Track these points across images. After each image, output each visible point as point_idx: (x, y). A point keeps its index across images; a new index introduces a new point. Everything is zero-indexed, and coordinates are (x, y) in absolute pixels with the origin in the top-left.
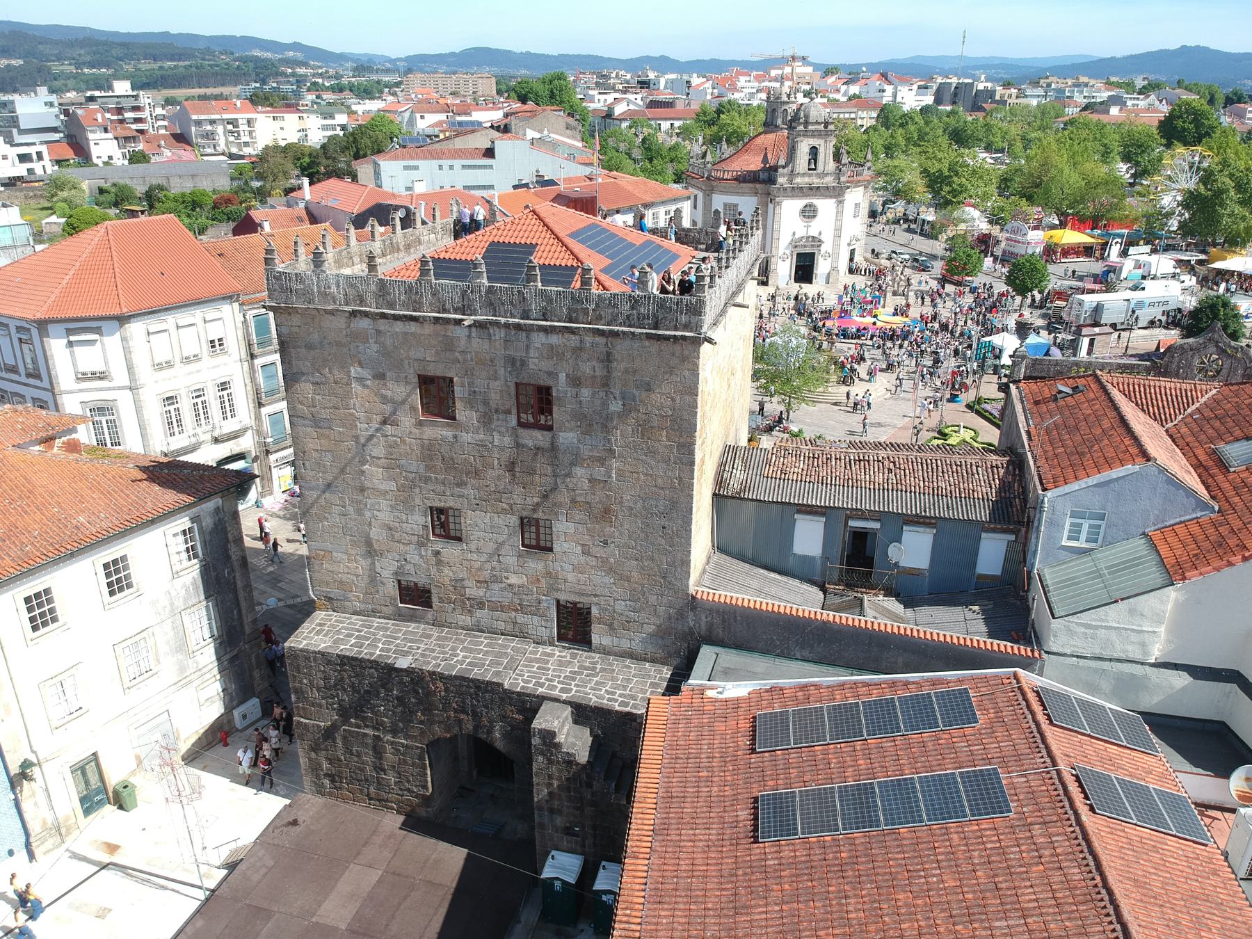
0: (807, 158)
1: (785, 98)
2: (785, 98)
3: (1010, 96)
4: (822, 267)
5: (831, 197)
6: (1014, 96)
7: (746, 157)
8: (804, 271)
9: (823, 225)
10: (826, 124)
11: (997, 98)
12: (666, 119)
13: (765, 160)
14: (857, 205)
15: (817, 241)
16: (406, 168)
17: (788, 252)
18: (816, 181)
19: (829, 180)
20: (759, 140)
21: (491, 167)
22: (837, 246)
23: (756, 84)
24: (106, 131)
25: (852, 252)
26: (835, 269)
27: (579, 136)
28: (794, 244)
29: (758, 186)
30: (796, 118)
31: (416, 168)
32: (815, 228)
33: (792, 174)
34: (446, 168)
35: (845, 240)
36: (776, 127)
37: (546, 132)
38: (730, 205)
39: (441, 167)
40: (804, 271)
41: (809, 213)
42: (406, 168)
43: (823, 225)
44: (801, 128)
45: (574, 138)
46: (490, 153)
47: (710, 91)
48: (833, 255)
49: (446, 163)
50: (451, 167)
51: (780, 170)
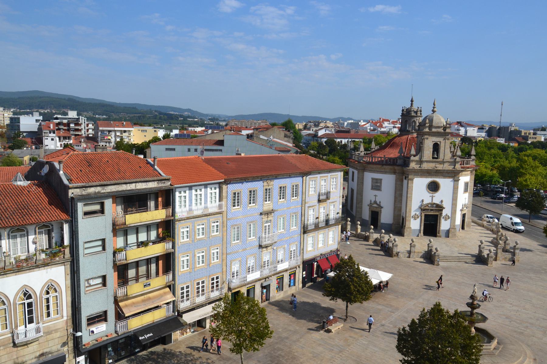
1: (413, 114)
2: (413, 114)
4: (444, 225)
5: (450, 177)
6: (532, 134)
7: (387, 150)
8: (431, 227)
9: (443, 196)
10: (445, 128)
11: (523, 134)
12: (345, 138)
13: (401, 152)
14: (466, 184)
15: (440, 208)
16: (167, 149)
17: (418, 213)
18: (440, 167)
19: (447, 167)
21: (221, 150)
22: (454, 211)
24: (54, 133)
25: (464, 216)
26: (453, 226)
27: (291, 141)
28: (422, 209)
29: (396, 168)
30: (422, 125)
31: (174, 149)
32: (437, 198)
33: (421, 162)
34: (192, 150)
35: (459, 207)
36: (408, 131)
37: (272, 137)
38: (377, 179)
39: (189, 150)
40: (431, 227)
41: (434, 187)
42: (167, 149)
43: (443, 196)
44: (427, 130)
45: (289, 142)
46: (221, 143)
47: (369, 128)
48: (452, 218)
49: (193, 147)
50: (196, 150)
51: (412, 158)
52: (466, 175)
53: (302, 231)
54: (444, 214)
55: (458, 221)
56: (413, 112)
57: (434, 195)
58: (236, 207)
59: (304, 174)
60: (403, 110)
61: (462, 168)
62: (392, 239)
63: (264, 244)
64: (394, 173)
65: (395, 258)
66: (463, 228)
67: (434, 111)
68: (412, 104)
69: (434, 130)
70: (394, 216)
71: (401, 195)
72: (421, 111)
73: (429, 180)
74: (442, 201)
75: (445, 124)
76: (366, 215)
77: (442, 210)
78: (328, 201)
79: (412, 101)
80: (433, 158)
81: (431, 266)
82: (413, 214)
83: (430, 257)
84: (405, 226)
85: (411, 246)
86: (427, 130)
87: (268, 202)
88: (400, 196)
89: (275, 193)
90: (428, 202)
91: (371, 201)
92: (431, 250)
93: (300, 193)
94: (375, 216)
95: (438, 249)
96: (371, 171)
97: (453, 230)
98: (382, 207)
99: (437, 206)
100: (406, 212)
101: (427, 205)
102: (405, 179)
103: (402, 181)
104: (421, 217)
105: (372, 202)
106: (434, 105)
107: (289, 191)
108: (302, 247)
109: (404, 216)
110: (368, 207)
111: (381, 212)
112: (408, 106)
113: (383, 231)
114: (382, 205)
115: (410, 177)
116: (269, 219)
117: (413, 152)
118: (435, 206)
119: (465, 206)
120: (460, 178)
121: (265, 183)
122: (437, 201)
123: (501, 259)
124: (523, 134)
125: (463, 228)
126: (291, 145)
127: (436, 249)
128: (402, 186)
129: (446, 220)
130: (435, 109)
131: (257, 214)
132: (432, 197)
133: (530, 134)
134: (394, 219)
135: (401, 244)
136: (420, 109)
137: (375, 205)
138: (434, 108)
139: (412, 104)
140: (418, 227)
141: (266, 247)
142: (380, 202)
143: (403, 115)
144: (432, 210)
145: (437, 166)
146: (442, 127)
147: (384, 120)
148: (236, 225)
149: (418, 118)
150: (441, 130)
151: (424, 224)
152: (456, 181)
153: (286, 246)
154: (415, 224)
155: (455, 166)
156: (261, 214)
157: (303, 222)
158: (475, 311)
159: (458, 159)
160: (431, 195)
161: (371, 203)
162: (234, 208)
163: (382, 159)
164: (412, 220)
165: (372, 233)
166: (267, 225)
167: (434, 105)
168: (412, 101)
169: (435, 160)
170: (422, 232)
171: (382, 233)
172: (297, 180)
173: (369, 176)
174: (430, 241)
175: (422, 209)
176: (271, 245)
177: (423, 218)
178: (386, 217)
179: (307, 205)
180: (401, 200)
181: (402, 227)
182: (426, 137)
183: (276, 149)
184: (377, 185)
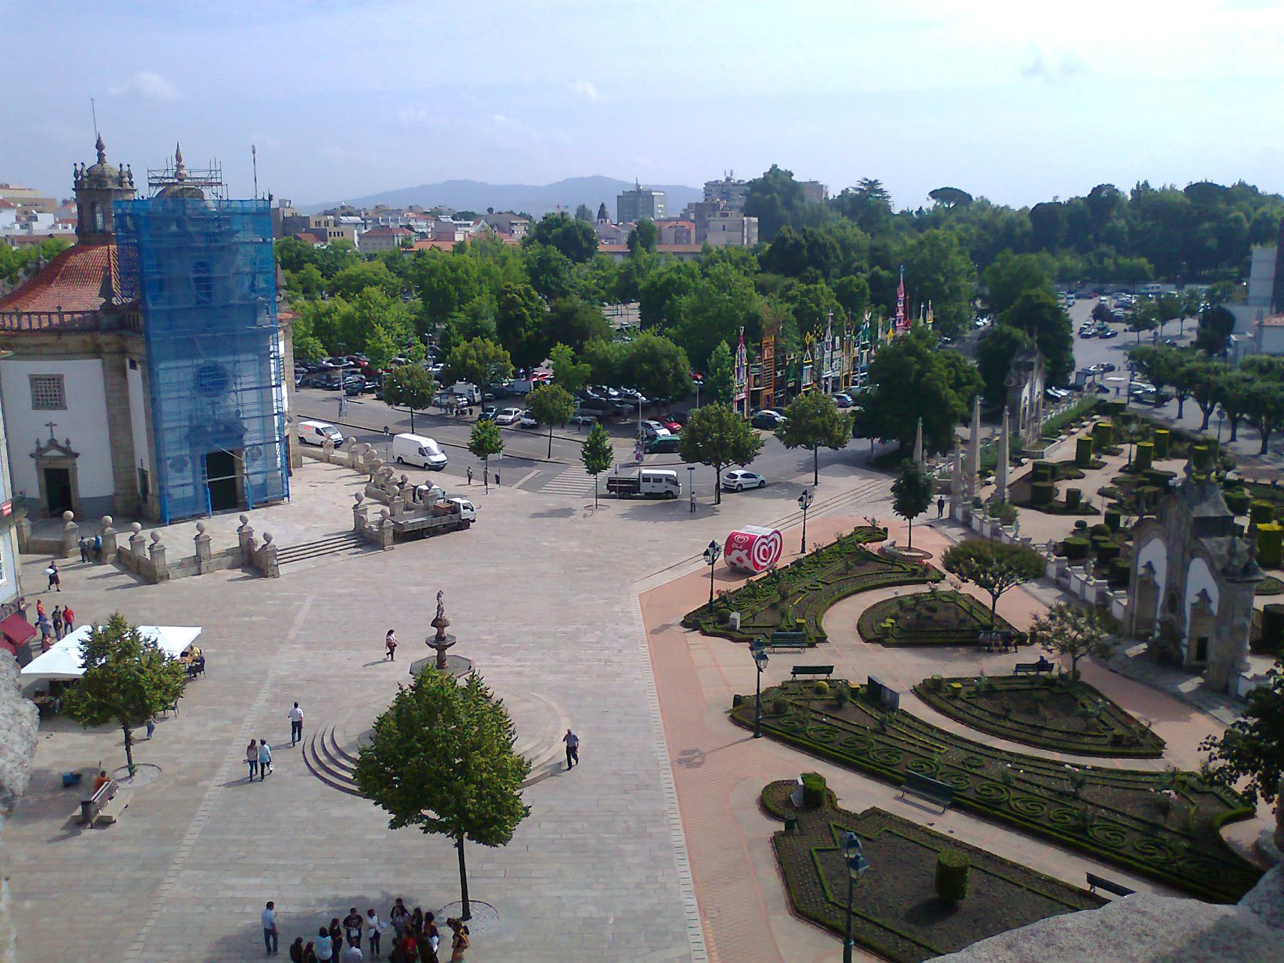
3: (327, 223)
6: (331, 224)
11: (313, 226)
20: (75, 260)
29: (103, 338)
38: (51, 379)
56: (110, 182)
57: (216, 399)
60: (76, 175)
64: (97, 352)
65: (162, 585)
68: (101, 156)
71: (127, 412)
72: (130, 176)
79: (99, 146)
81: (263, 581)
83: (253, 560)
91: (38, 442)
92: (251, 543)
95: (273, 533)
98: (76, 455)
105: (44, 444)
110: (33, 461)
112: (92, 161)
113: (110, 518)
114: (74, 449)
118: (222, 427)
124: (313, 226)
127: (266, 537)
132: (213, 404)
133: (327, 223)
134: (116, 479)
136: (125, 168)
139: (101, 156)
142: (68, 441)
143: (78, 187)
158: (448, 652)
161: (39, 449)
163: (56, 320)
165: (73, 531)
168: (99, 146)
171: (106, 525)
174: (242, 518)
181: (145, 500)
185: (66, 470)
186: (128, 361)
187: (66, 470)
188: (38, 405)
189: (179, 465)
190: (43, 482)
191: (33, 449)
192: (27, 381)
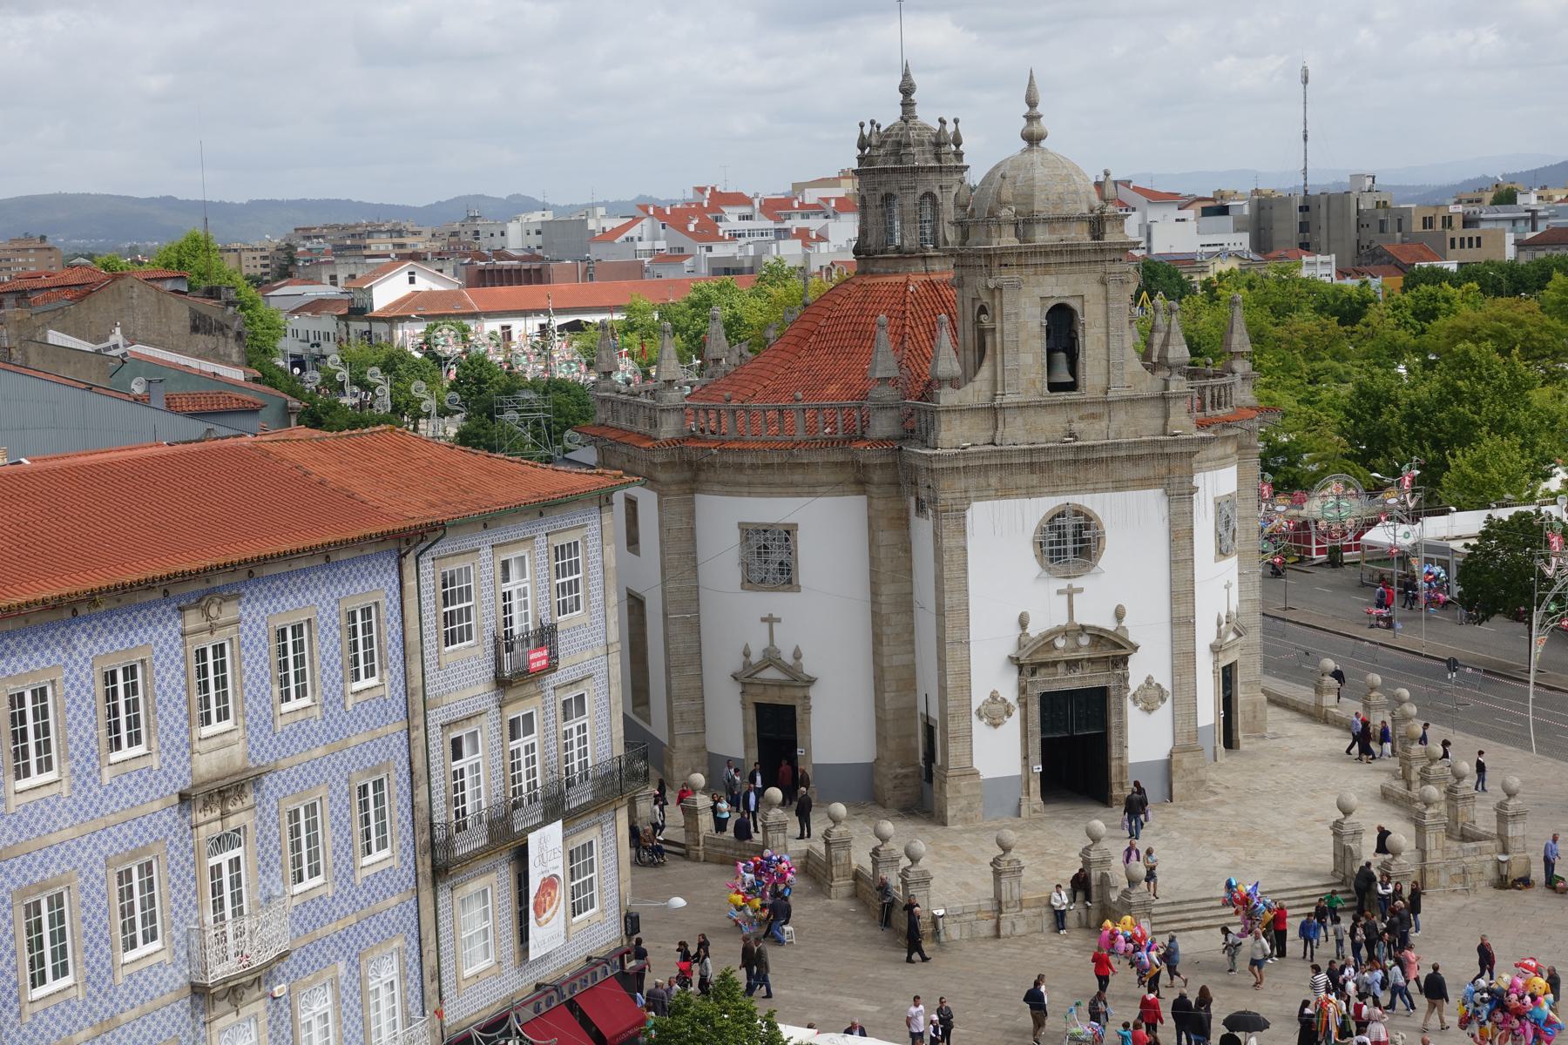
0: (1039, 345)
1: (922, 158)
4: (1143, 739)
5: (1144, 483)
6: (1457, 223)
9: (1125, 584)
10: (1097, 224)
12: (525, 314)
15: (1113, 650)
18: (1093, 433)
22: (1183, 660)
23: (770, 224)
25: (1228, 676)
27: (235, 352)
28: (1027, 665)
35: (1205, 634)
37: (117, 337)
41: (1070, 544)
43: (1125, 584)
45: (222, 359)
51: (947, 397)
52: (1222, 462)
53: (426, 868)
54: (1135, 681)
55: (1208, 713)
57: (1076, 583)
58: (36, 779)
59: (407, 542)
61: (1201, 425)
62: (896, 847)
63: (218, 972)
64: (861, 484)
66: (1230, 742)
67: (1033, 139)
68: (908, 105)
69: (1042, 236)
70: (880, 721)
71: (906, 604)
72: (957, 141)
73: (1045, 505)
74: (1119, 614)
75: (1097, 202)
76: (731, 735)
77: (1124, 660)
78: (552, 680)
79: (907, 90)
80: (1054, 387)
82: (979, 698)
84: (945, 767)
85: (997, 874)
86: (1008, 240)
87: (216, 727)
88: (905, 611)
89: (251, 664)
90: (1053, 625)
91: (747, 654)
93: (394, 653)
94: (777, 729)
96: (732, 488)
97: (1187, 760)
98: (811, 681)
99: (1099, 637)
100: (943, 689)
101: (1048, 641)
102: (920, 508)
103: (902, 523)
104: (1024, 706)
105: (755, 658)
106: (1032, 103)
107: (326, 648)
108: (430, 960)
109: (934, 714)
111: (807, 709)
112: (889, 116)
113: (840, 809)
114: (809, 667)
115: (946, 497)
116: (233, 822)
117: (947, 363)
119: (1233, 625)
120: (1199, 479)
121: (193, 620)
122: (1094, 612)
123: (1444, 878)
125: (1230, 742)
126: (237, 375)
128: (907, 548)
129: (1149, 710)
130: (1036, 128)
131: (158, 804)
132: (1070, 593)
134: (881, 738)
135: (949, 873)
136: (950, 128)
137: (771, 674)
138: (1031, 118)
139: (908, 105)
140: (1014, 768)
141: (233, 992)
144: (1072, 664)
145: (1076, 427)
146: (1080, 219)
147: (722, 199)
148: (43, 887)
149: (946, 180)
150: (1080, 235)
151: (1043, 741)
152: (1181, 496)
153: (342, 967)
154: (998, 752)
155: (1166, 417)
156: (184, 797)
157: (421, 816)
159: (1179, 384)
160: (1063, 584)
161: (747, 665)
162: (23, 784)
164: (979, 727)
166: (223, 858)
167: (1032, 103)
168: (907, 90)
169: (1063, 396)
170: (1035, 786)
172: (373, 587)
173: (724, 517)
175: (1021, 667)
176: (260, 978)
177: (1035, 710)
178: (837, 733)
179: (437, 717)
180: (910, 629)
181: (929, 777)
182: (1004, 277)
183: (171, 406)
184: (771, 560)
185: (793, 708)
186: (913, 500)
187: (791, 709)
188: (749, 583)
189: (994, 714)
190: (753, 729)
191: (737, 664)
192: (735, 537)
